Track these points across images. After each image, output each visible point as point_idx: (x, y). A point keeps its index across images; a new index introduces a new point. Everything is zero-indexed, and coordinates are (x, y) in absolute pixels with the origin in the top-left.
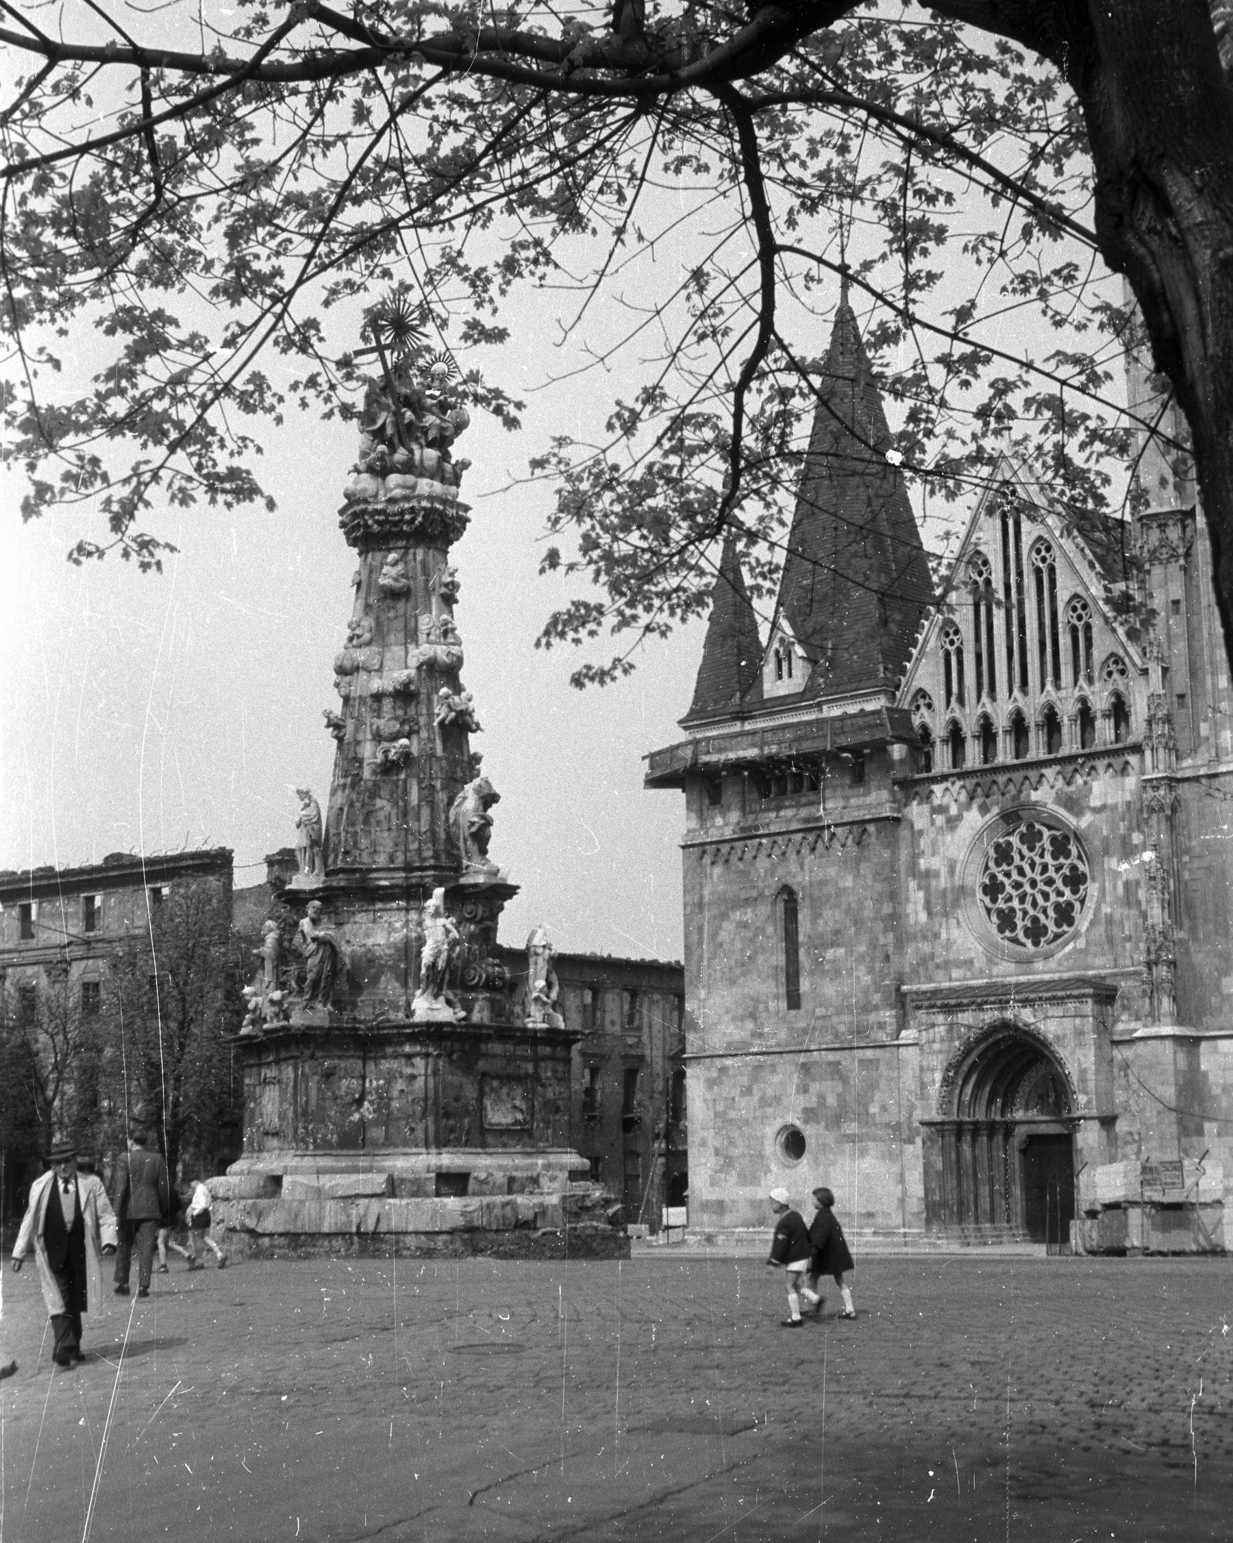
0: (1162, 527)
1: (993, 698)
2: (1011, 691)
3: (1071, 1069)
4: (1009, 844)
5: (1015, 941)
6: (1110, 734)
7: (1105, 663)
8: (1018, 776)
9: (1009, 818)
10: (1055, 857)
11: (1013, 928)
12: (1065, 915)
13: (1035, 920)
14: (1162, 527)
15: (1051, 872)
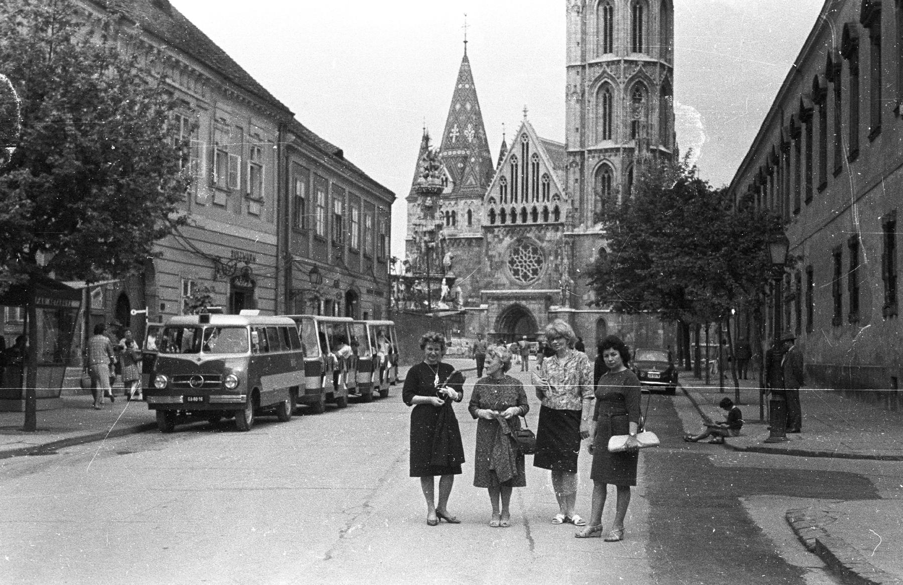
0: (574, 156)
1: (516, 201)
2: (522, 201)
3: (537, 319)
4: (519, 249)
5: (519, 279)
6: (554, 218)
7: (553, 196)
8: (523, 229)
9: (519, 241)
10: (533, 254)
11: (519, 275)
12: (535, 272)
13: (525, 273)
14: (574, 156)
15: (531, 259)
